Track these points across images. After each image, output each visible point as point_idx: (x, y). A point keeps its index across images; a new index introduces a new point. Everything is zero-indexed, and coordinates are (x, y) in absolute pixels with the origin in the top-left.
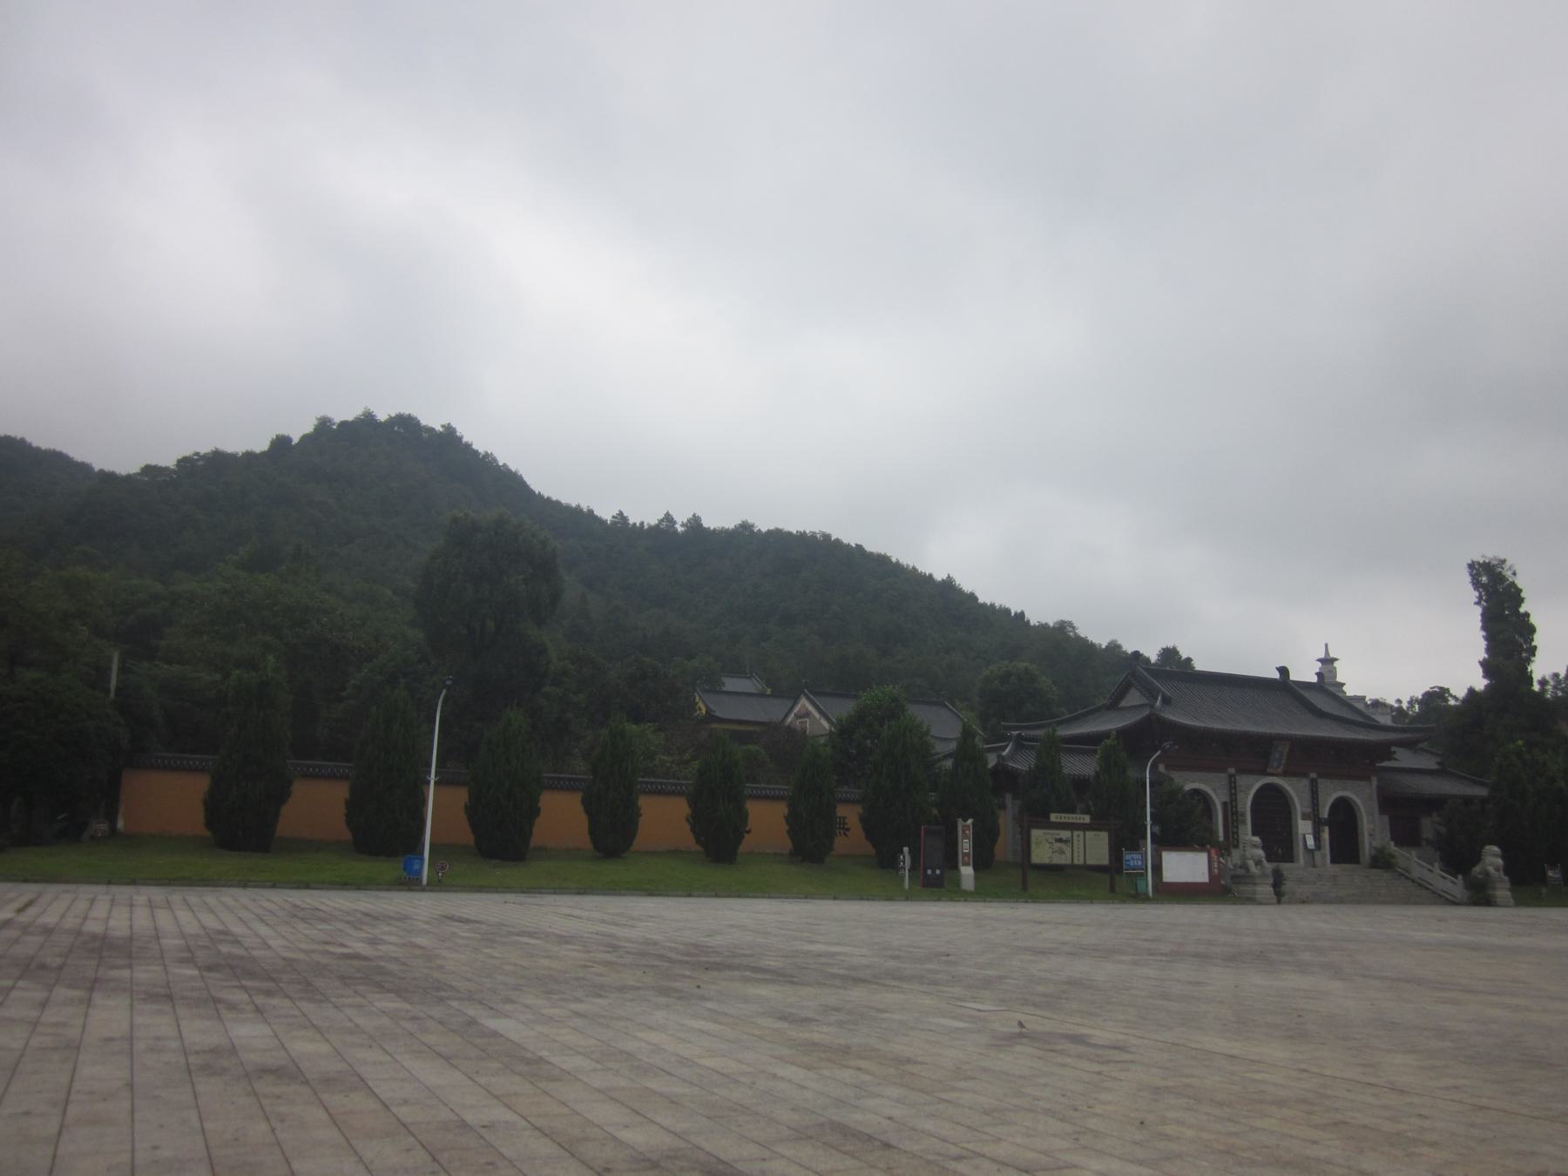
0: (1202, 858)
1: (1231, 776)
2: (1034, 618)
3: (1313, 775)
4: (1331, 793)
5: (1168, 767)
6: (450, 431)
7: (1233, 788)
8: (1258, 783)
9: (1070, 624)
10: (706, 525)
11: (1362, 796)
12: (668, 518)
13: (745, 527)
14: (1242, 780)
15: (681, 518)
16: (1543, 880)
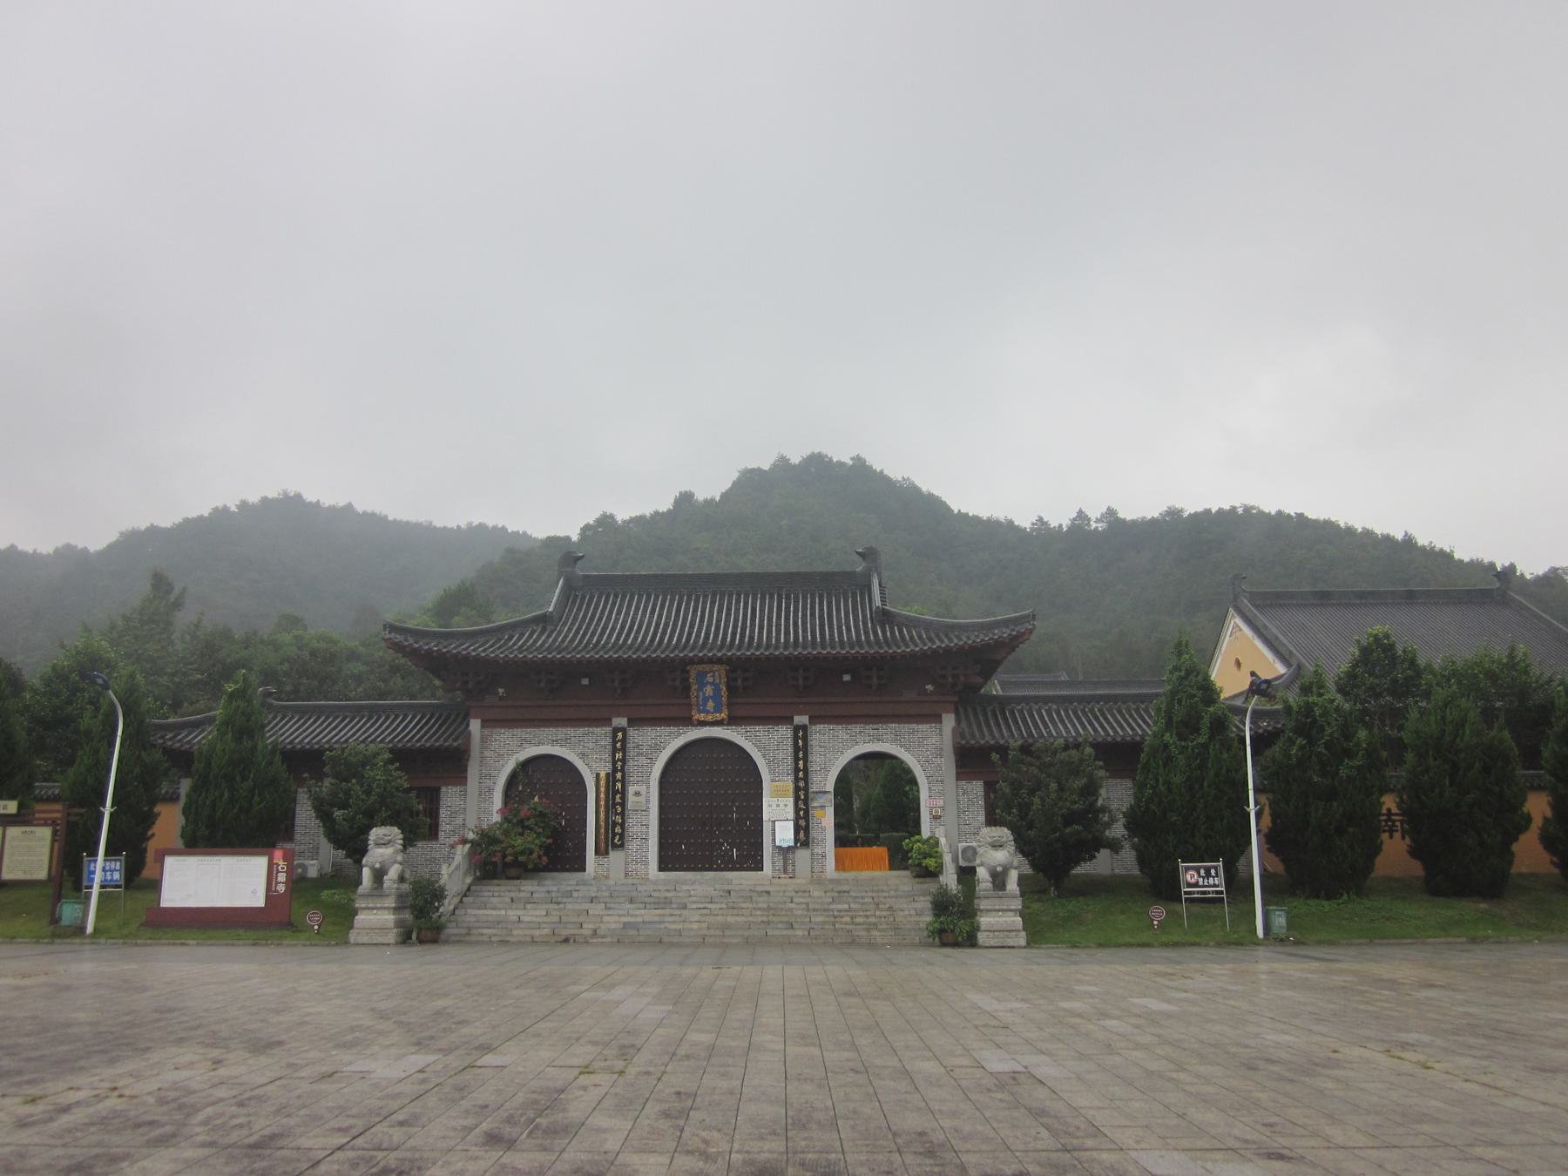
0: (259, 864)
1: (616, 731)
2: (390, 518)
3: (798, 720)
4: (838, 749)
5: (486, 723)
6: (859, 462)
7: (619, 747)
8: (676, 739)
10: (1121, 515)
11: (924, 750)
13: (1174, 513)
14: (642, 737)
15: (1094, 512)
16: (1165, 888)
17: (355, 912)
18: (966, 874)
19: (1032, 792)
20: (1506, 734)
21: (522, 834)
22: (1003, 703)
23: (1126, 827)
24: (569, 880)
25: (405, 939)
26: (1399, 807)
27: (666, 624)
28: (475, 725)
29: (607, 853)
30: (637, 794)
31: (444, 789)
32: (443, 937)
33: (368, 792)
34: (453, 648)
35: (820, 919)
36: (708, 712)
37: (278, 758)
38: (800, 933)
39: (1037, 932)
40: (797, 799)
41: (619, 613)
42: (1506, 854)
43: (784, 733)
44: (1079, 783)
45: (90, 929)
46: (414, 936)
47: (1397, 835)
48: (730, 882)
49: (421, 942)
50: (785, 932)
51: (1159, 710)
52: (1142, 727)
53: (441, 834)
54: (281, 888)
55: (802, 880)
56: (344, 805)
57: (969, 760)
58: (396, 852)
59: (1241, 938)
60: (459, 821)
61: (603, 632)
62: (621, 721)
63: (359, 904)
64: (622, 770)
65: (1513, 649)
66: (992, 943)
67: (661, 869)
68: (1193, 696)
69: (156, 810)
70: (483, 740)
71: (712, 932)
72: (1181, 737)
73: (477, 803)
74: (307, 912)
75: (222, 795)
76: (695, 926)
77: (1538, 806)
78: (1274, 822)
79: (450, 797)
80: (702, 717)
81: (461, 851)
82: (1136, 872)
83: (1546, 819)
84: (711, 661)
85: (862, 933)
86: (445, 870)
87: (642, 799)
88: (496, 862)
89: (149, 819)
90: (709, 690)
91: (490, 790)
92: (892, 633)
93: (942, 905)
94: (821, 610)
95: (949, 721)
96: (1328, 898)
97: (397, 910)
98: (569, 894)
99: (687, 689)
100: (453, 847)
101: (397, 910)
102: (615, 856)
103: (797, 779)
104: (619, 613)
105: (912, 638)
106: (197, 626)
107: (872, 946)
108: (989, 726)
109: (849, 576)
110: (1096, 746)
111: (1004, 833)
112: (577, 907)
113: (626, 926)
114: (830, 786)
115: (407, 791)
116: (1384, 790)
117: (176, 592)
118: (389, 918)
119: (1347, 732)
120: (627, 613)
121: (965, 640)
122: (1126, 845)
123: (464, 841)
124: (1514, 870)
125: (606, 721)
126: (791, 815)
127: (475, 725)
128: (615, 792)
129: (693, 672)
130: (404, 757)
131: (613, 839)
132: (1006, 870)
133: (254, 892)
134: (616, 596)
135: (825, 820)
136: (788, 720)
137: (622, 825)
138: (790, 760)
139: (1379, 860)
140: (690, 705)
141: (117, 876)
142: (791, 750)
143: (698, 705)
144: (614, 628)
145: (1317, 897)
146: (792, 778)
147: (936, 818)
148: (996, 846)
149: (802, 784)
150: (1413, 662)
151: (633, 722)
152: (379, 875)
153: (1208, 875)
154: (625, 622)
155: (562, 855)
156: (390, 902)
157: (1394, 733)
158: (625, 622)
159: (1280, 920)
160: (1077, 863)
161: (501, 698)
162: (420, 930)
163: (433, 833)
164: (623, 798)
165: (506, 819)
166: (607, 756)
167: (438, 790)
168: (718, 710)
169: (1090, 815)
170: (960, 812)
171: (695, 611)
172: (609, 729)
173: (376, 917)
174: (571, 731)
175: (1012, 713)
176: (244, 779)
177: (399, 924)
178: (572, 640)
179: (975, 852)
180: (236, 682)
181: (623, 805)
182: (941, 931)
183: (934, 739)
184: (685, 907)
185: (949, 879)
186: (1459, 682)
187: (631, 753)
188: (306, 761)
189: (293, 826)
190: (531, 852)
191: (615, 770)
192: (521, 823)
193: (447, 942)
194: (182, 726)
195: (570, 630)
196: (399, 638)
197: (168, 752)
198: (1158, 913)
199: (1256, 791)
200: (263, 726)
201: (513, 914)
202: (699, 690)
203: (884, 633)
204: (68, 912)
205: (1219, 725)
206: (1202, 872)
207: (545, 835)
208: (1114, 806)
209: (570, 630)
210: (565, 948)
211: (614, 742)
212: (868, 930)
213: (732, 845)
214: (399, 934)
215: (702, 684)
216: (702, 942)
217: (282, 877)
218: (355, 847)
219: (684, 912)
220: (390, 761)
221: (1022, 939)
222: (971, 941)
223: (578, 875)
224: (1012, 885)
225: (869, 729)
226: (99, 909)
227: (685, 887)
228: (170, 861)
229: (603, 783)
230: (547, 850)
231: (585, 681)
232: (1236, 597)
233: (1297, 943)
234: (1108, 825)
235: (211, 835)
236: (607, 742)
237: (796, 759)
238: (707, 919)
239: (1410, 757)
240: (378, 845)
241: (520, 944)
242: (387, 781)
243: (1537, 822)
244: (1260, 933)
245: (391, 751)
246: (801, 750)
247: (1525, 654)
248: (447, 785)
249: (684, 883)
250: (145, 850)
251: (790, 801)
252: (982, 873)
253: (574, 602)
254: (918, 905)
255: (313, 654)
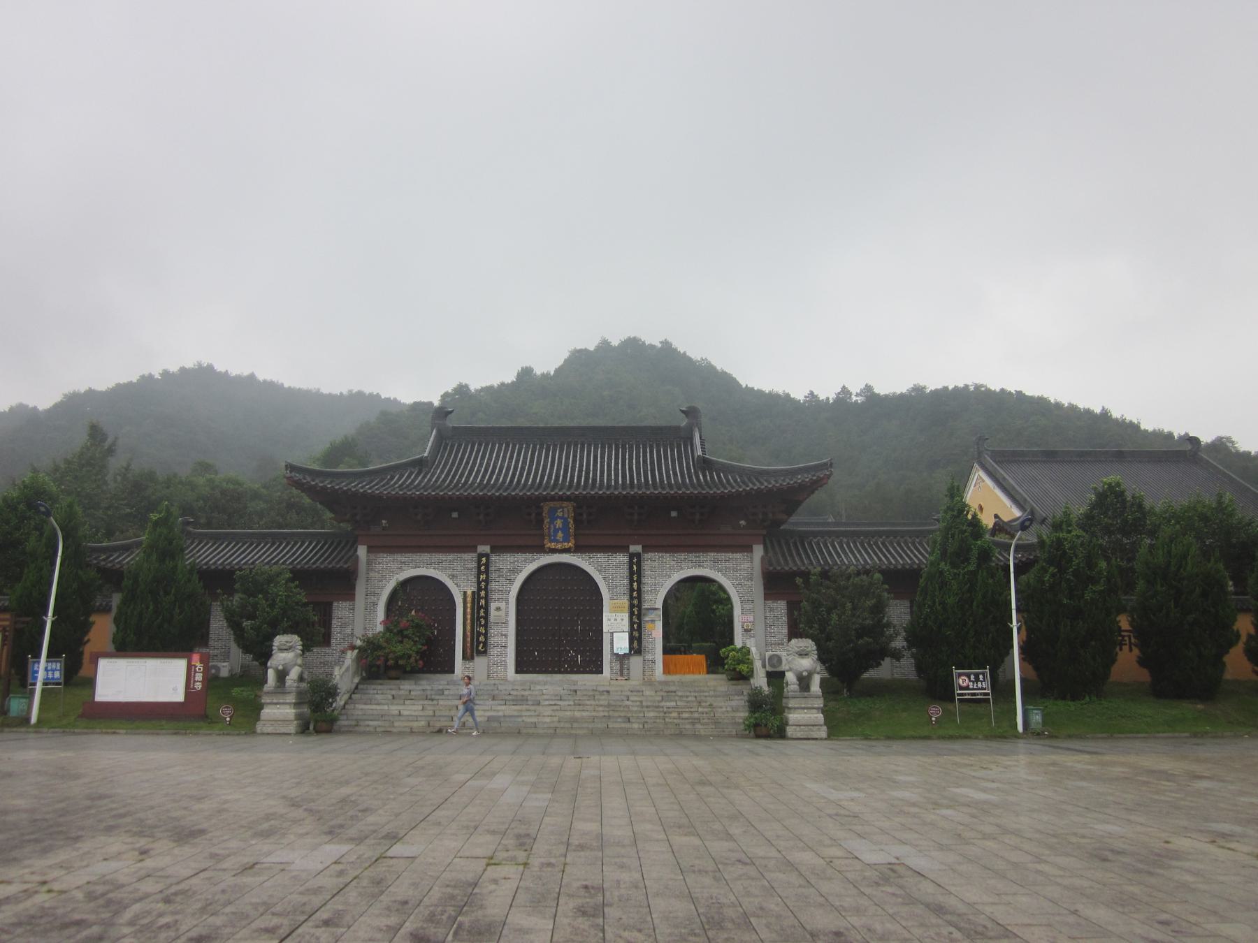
1: (481, 556)
4: (665, 574)
5: (371, 549)
6: (667, 345)
7: (483, 571)
8: (531, 564)
9: (1229, 439)
10: (876, 391)
11: (737, 576)
12: (844, 390)
13: (918, 390)
14: (503, 562)
15: (855, 388)
16: (942, 691)
17: (261, 707)
18: (776, 677)
19: (829, 611)
20: (1221, 566)
21: (401, 642)
22: (803, 537)
23: (906, 639)
24: (440, 681)
25: (304, 729)
26: (1131, 624)
27: (523, 468)
28: (362, 551)
29: (472, 658)
30: (498, 609)
31: (335, 604)
32: (335, 727)
33: (272, 606)
34: (344, 486)
35: (652, 714)
36: (558, 542)
37: (195, 577)
38: (636, 726)
39: (837, 726)
40: (631, 614)
41: (483, 458)
42: (1218, 663)
43: (621, 560)
44: (870, 603)
45: (34, 719)
46: (311, 727)
47: (1126, 648)
48: (575, 683)
49: (318, 731)
50: (623, 725)
51: (935, 542)
52: (918, 556)
53: (333, 641)
54: (198, 686)
55: (635, 681)
56: (251, 617)
57: (776, 583)
58: (297, 656)
59: (1004, 733)
60: (348, 630)
61: (470, 474)
62: (484, 549)
63: (265, 700)
64: (486, 589)
65: (1220, 496)
66: (799, 735)
67: (517, 672)
68: (964, 532)
69: (92, 619)
70: (369, 563)
71: (562, 725)
72: (954, 565)
73: (364, 616)
74: (220, 707)
75: (148, 608)
76: (548, 720)
77: (1244, 625)
78: (1028, 636)
79: (340, 610)
80: (553, 545)
81: (350, 656)
82: (913, 676)
83: (1249, 636)
84: (561, 498)
85: (688, 726)
86: (337, 672)
87: (502, 613)
88: (379, 665)
89: (86, 627)
90: (559, 523)
91: (375, 605)
92: (712, 477)
93: (756, 703)
94: (652, 457)
95: (758, 551)
96: (1073, 699)
97: (296, 705)
98: (441, 692)
99: (540, 522)
100: (343, 652)
101: (296, 705)
102: (480, 661)
103: (631, 598)
104: (483, 458)
105: (728, 481)
106: (126, 469)
107: (697, 737)
108: (791, 555)
109: (677, 429)
110: (882, 572)
111: (808, 644)
112: (450, 703)
113: (490, 719)
114: (659, 604)
115: (306, 605)
116: (1122, 610)
117: (110, 441)
118: (290, 712)
119: (1090, 564)
120: (490, 459)
121: (773, 483)
122: (907, 654)
123: (353, 648)
124: (1228, 676)
125: (472, 548)
126: (627, 628)
127: (362, 551)
128: (480, 607)
129: (546, 507)
130: (301, 576)
131: (478, 646)
132: (810, 675)
133: (175, 689)
134: (480, 445)
135: (655, 632)
136: (623, 548)
137: (486, 635)
138: (626, 582)
139: (1115, 669)
140: (542, 536)
141: (57, 675)
142: (626, 574)
143: (549, 536)
144: (479, 471)
145: (1064, 698)
146: (627, 597)
147: (747, 631)
148: (803, 654)
149: (636, 602)
150: (1140, 506)
151: (494, 549)
152: (282, 675)
153: (977, 680)
154: (488, 465)
155: (435, 659)
156: (291, 698)
157: (1124, 564)
158: (488, 465)
159: (1036, 718)
160: (866, 669)
161: (384, 529)
162: (316, 721)
163: (326, 641)
164: (487, 612)
165: (387, 629)
166: (473, 577)
167: (330, 605)
168: (566, 539)
169: (878, 628)
170: (767, 626)
171: (546, 457)
172: (475, 555)
173: (279, 712)
174: (442, 556)
175: (810, 544)
176: (167, 593)
177: (299, 717)
178: (439, 481)
179: (780, 660)
180: (160, 513)
181: (486, 618)
182: (756, 725)
183: (746, 566)
184: (539, 704)
185: (760, 680)
186: (1178, 523)
187: (493, 575)
188: (219, 580)
189: (208, 634)
190: (410, 657)
191: (480, 589)
192: (400, 632)
193: (339, 732)
194: (115, 549)
195: (442, 472)
196: (298, 476)
197: (102, 570)
198: (936, 711)
199: (1018, 610)
200: (182, 550)
201: (394, 709)
202: (552, 522)
203: (705, 476)
204: (16, 705)
205: (985, 555)
206: (972, 677)
207: (420, 643)
208: (895, 622)
209: (442, 472)
210: (438, 739)
211: (479, 566)
212: (693, 724)
213: (577, 652)
214: (299, 725)
215: (553, 519)
216: (554, 734)
217: (199, 677)
218: (263, 654)
219: (539, 708)
220: (292, 580)
221: (823, 733)
222: (780, 734)
223: (448, 677)
224: (815, 687)
225: (692, 557)
226: (41, 704)
227: (539, 687)
228: (103, 664)
229: (469, 599)
230: (422, 654)
231: (455, 515)
232: (980, 453)
233: (1051, 737)
234: (891, 638)
235: (138, 641)
236: (473, 565)
237: (631, 581)
238: (557, 714)
239: (1141, 585)
240: (281, 650)
241: (401, 734)
242: (288, 596)
243: (1244, 638)
244: (1020, 728)
245: (292, 571)
246: (635, 574)
247: (1231, 500)
248: (338, 600)
249: (538, 683)
250: (82, 653)
251: (626, 616)
252: (790, 677)
253: (445, 448)
254: (734, 703)
255: (224, 492)
